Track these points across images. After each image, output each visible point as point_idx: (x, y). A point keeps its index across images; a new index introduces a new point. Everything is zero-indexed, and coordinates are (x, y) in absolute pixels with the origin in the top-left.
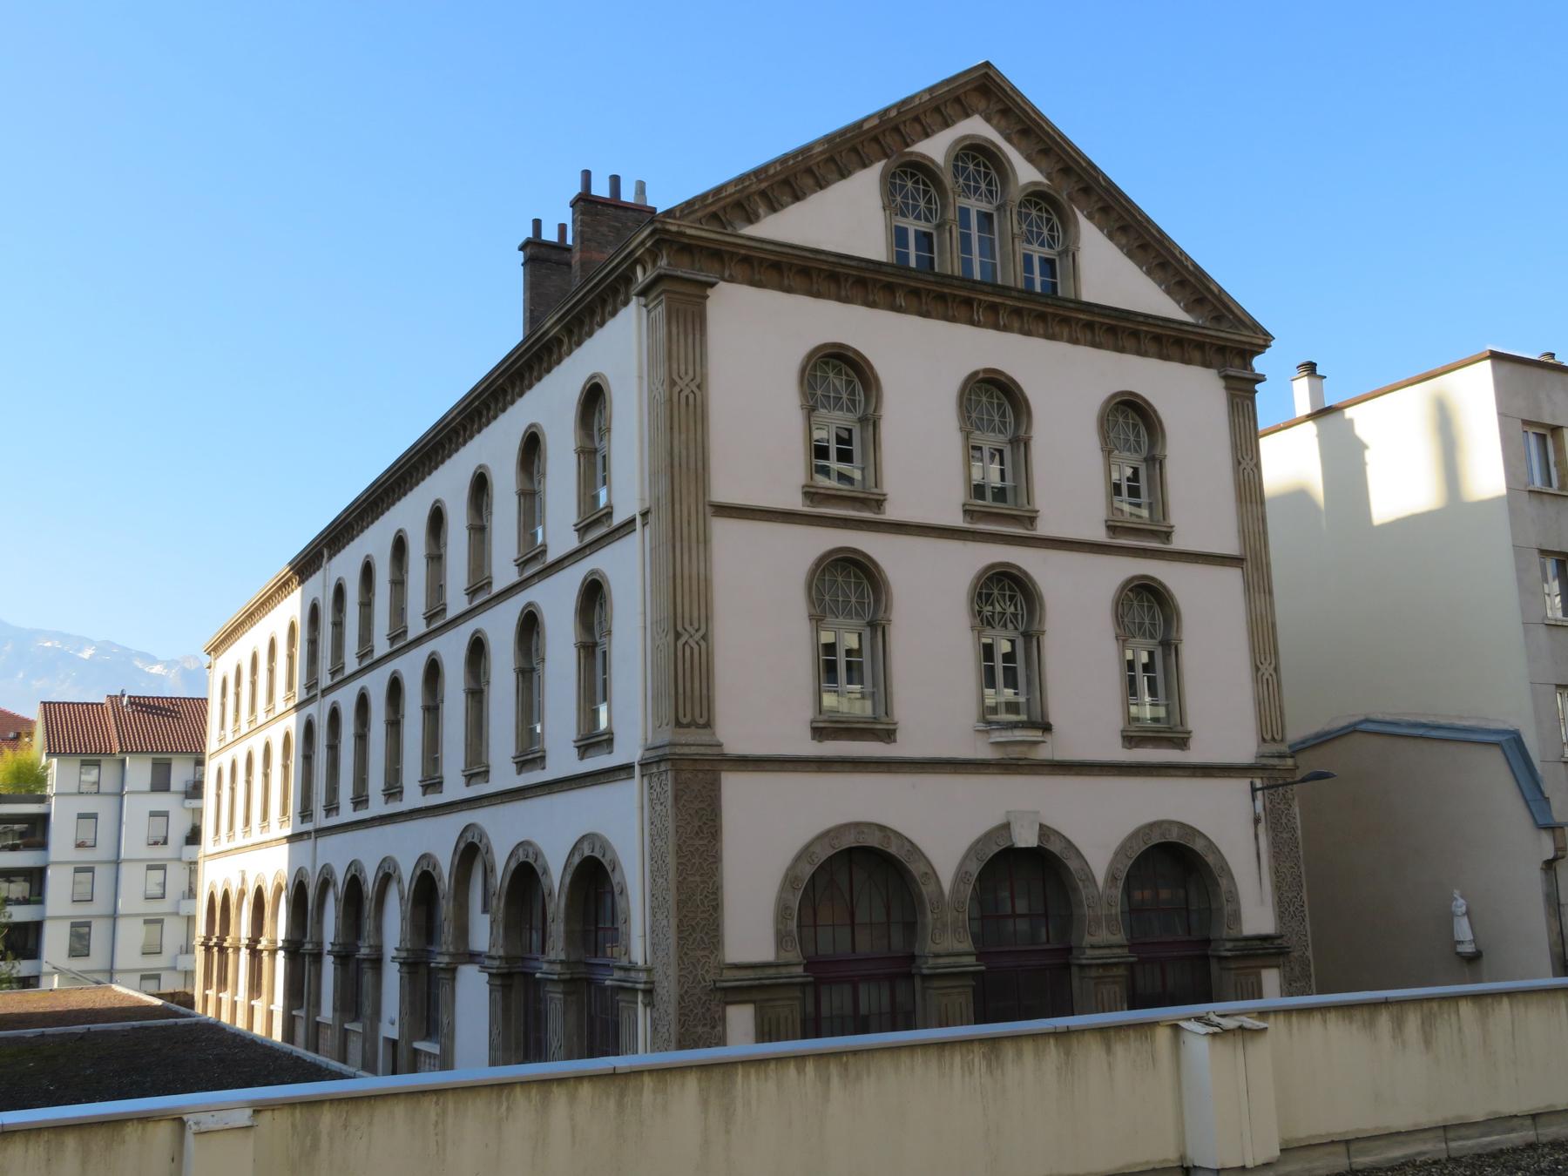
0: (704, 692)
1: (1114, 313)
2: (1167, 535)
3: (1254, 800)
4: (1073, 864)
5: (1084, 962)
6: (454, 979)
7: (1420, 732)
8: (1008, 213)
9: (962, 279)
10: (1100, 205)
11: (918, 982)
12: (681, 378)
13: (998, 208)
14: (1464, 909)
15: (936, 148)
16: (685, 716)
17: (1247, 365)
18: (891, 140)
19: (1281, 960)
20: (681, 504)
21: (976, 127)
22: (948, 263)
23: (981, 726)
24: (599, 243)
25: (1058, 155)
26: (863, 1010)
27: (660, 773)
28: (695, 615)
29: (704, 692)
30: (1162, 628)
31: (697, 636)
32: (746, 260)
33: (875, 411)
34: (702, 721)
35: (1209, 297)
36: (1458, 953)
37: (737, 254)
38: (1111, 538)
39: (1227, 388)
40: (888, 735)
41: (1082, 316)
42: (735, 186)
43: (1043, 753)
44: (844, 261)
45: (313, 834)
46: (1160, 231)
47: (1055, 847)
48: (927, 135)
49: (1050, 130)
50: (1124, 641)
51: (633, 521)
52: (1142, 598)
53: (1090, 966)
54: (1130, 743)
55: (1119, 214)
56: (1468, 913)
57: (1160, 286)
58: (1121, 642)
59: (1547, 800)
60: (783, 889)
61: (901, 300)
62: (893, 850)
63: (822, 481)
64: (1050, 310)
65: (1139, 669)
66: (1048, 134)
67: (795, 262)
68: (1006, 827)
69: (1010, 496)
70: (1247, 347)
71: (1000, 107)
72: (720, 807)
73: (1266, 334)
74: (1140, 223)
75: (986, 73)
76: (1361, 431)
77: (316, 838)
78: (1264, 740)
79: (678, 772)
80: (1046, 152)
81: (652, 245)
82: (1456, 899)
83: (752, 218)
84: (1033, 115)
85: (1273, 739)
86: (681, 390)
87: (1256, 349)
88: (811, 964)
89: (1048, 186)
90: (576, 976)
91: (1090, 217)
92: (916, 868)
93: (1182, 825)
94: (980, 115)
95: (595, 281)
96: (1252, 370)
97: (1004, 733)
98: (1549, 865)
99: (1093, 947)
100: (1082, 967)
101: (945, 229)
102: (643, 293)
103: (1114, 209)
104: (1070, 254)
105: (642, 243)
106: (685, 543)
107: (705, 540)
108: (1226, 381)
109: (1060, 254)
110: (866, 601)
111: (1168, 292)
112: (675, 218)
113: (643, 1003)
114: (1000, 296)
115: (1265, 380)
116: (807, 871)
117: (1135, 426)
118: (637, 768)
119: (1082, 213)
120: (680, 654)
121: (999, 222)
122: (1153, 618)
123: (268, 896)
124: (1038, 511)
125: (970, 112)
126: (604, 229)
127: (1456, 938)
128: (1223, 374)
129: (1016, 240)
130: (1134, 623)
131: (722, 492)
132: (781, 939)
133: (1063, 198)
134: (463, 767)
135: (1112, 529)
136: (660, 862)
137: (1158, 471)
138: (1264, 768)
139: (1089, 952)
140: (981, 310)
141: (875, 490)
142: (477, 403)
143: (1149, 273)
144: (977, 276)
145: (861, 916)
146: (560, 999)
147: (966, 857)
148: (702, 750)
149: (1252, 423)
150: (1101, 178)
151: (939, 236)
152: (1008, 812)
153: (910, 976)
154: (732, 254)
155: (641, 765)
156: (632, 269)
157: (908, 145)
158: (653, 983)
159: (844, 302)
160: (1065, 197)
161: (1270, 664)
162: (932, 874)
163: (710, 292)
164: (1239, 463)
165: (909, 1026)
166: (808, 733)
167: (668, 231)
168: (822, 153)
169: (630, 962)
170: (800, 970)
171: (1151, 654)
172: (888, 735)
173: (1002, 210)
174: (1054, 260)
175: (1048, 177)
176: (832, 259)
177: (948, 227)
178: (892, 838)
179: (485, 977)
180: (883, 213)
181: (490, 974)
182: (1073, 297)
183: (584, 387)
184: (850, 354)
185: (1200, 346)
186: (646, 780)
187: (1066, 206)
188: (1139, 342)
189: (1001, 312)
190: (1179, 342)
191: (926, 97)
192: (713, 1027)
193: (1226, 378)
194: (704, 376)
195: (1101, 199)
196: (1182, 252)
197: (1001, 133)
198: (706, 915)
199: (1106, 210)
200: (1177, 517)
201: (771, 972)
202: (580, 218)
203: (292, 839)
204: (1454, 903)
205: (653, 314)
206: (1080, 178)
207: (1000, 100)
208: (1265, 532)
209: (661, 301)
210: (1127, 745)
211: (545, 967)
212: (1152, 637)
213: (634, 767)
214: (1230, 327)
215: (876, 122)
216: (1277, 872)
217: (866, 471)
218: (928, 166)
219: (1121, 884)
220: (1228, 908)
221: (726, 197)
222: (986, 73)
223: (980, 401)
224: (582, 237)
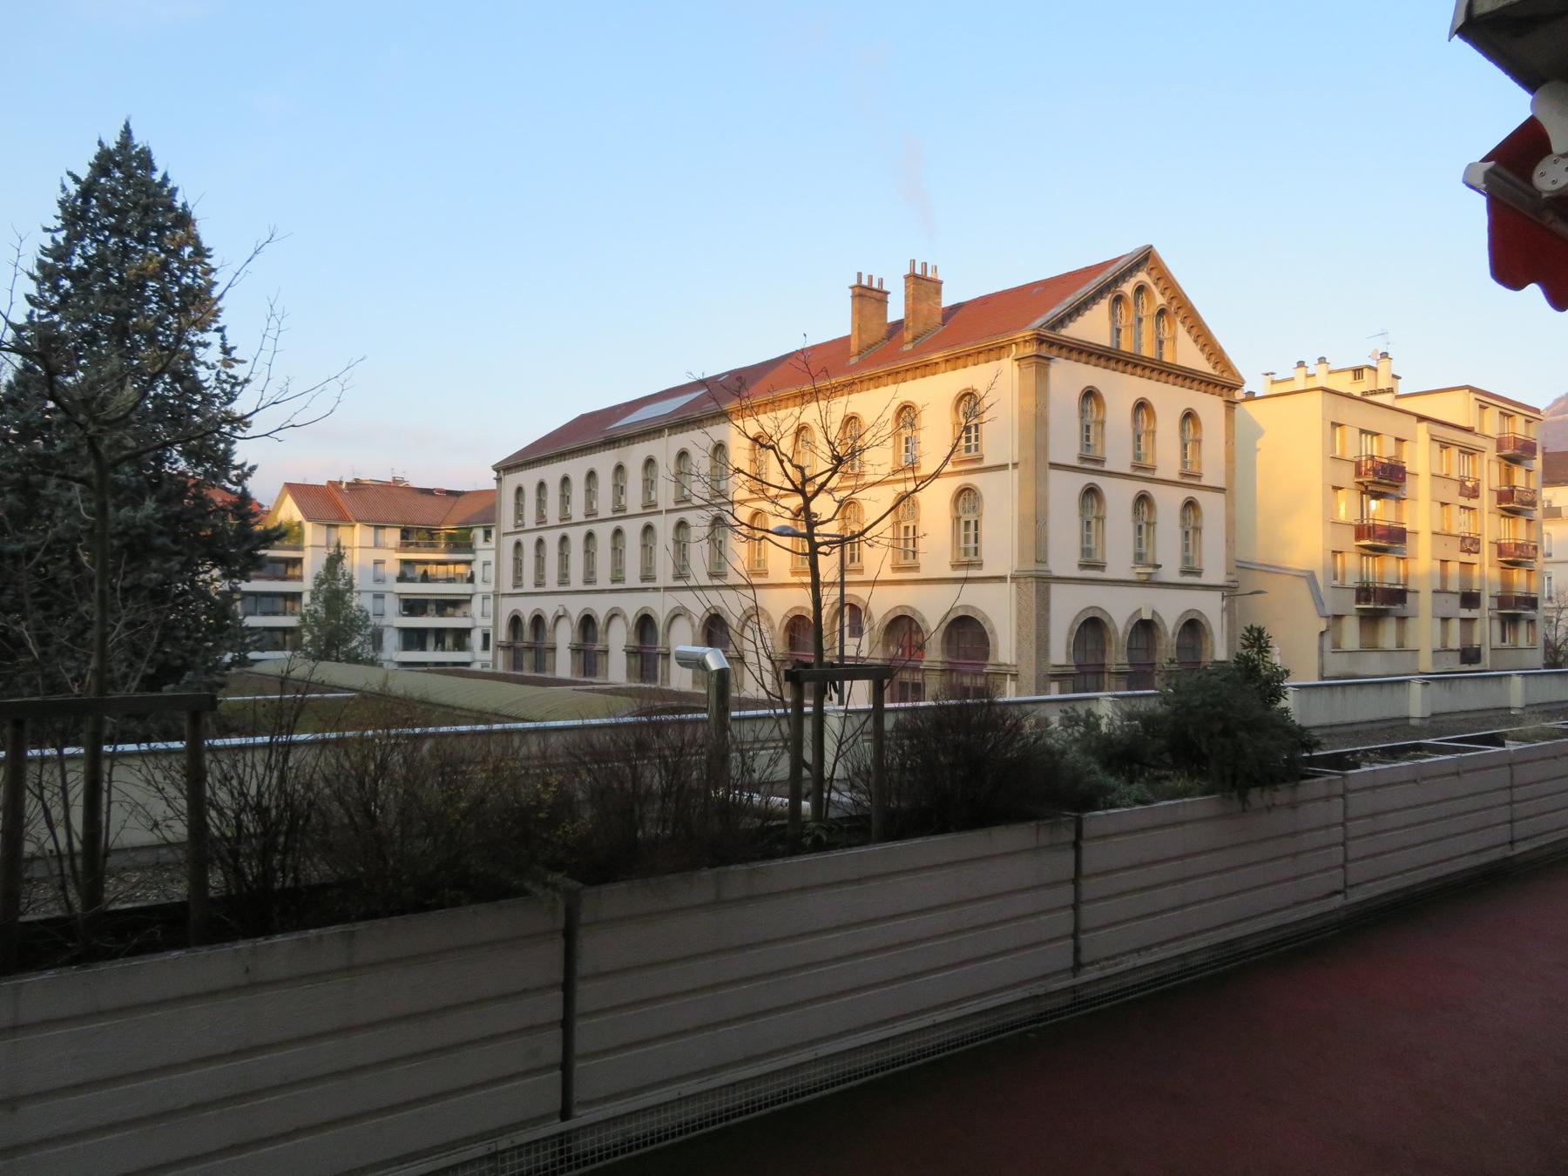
11: (1106, 676)
15: (1128, 288)
22: (1126, 346)
39: (1227, 407)
47: (1156, 620)
56: (1279, 654)
59: (1323, 604)
68: (1140, 610)
79: (1037, 582)
88: (1078, 666)
98: (1322, 634)
118: (1009, 579)
126: (922, 293)
138: (1227, 587)
145: (1088, 648)
148: (1044, 573)
162: (1116, 630)
170: (1074, 668)
186: (1014, 585)
201: (1065, 669)
211: (925, 663)
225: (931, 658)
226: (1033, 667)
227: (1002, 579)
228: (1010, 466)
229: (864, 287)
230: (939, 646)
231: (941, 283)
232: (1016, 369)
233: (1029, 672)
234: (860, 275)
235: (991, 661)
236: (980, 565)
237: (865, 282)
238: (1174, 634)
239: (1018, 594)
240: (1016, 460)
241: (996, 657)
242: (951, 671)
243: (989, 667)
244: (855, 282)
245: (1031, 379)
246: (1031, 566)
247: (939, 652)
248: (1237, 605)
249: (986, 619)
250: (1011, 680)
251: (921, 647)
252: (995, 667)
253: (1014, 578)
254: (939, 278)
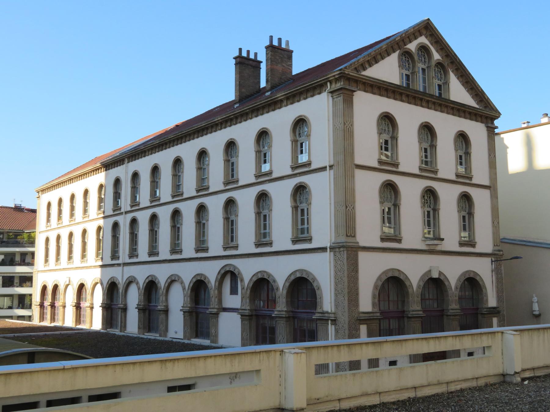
1: (460, 105)
2: (470, 178)
3: (492, 264)
4: (446, 283)
5: (449, 314)
6: (218, 317)
7: (524, 243)
8: (431, 69)
9: (423, 93)
10: (456, 68)
11: (406, 319)
12: (346, 122)
13: (428, 67)
14: (537, 300)
15: (412, 46)
16: (349, 233)
17: (493, 123)
18: (401, 44)
19: (498, 315)
21: (423, 40)
23: (424, 239)
24: (276, 62)
25: (446, 50)
26: (391, 327)
27: (340, 251)
30: (433, 204)
31: (352, 208)
32: (364, 83)
33: (397, 135)
34: (353, 235)
35: (484, 100)
36: (533, 315)
37: (362, 81)
38: (421, 173)
39: (488, 130)
40: (399, 241)
41: (452, 105)
42: (363, 59)
43: (439, 248)
44: (391, 85)
45: (122, 265)
46: (472, 77)
47: (442, 278)
48: (410, 42)
49: (444, 42)
50: (460, 212)
51: (326, 167)
52: (388, 188)
53: (450, 315)
56: (537, 302)
57: (470, 95)
58: (459, 213)
60: (374, 289)
61: (404, 98)
62: (401, 277)
63: (383, 158)
64: (443, 103)
65: (386, 213)
66: (443, 43)
67: (378, 85)
68: (430, 271)
69: (429, 163)
70: (494, 117)
71: (430, 33)
72: (358, 262)
73: (500, 113)
75: (428, 22)
76: (506, 142)
77: (123, 266)
78: (495, 245)
79: (348, 251)
80: (442, 49)
81: (338, 77)
82: (534, 297)
83: (365, 69)
84: (440, 37)
85: (497, 245)
86: (347, 126)
87: (496, 118)
88: (382, 313)
89: (442, 61)
90: (290, 316)
91: (453, 72)
92: (407, 283)
93: (474, 272)
94: (424, 35)
95: (308, 84)
96: (494, 125)
97: (431, 241)
99: (452, 309)
100: (447, 315)
101: (414, 74)
102: (332, 92)
103: (460, 70)
104: (447, 84)
105: (334, 76)
107: (353, 177)
109: (443, 83)
110: (392, 197)
111: (473, 97)
112: (347, 69)
113: (331, 324)
114: (431, 98)
115: (498, 128)
116: (380, 283)
117: (388, 125)
118: (328, 249)
119: (451, 70)
120: (347, 213)
121: (428, 72)
122: (466, 205)
123: (61, 288)
124: (473, 176)
125: (422, 35)
127: (533, 309)
128: (487, 126)
129: (434, 79)
130: (385, 197)
131: (358, 161)
132: (374, 305)
133: (446, 65)
134: (222, 244)
135: (458, 176)
136: (340, 279)
137: (469, 157)
138: (495, 254)
139: (451, 311)
140: (424, 102)
141: (396, 161)
142: (232, 117)
143: (468, 91)
144: (404, 85)
145: (390, 299)
146: (284, 323)
147: (420, 281)
148: (354, 244)
150: (457, 59)
151: (412, 76)
152: (431, 267)
153: (403, 317)
154: (360, 81)
155: (330, 248)
156: (326, 83)
157: (405, 45)
158: (336, 317)
159: (417, 106)
160: (446, 64)
161: (497, 221)
162: (411, 285)
163: (354, 93)
164: (490, 155)
165: (477, 328)
166: (379, 240)
167: (345, 73)
168: (385, 48)
169: (323, 311)
170: (378, 314)
171: (389, 209)
172: (399, 241)
173: (429, 68)
174: (409, 75)
175: (442, 58)
176: (388, 84)
177: (415, 74)
179: (239, 316)
180: (398, 68)
181: (241, 315)
182: (448, 98)
183: (296, 119)
184: (390, 115)
185: (481, 116)
186: (332, 253)
187: (446, 67)
188: (365, 86)
189: (430, 103)
190: (476, 115)
191: (412, 30)
192: (357, 331)
193: (487, 127)
194: (353, 122)
195: (456, 65)
196: (478, 85)
197: (430, 42)
198: (355, 296)
200: (474, 172)
201: (372, 315)
202: (270, 53)
203: (102, 266)
204: (533, 298)
205: (335, 99)
206: (451, 59)
207: (431, 31)
208: (496, 178)
209: (341, 96)
210: (460, 246)
211: (276, 313)
212: (465, 211)
213: (327, 248)
214: (489, 110)
216: (497, 287)
217: (393, 155)
218: (410, 53)
219: (458, 290)
220: (485, 298)
221: (360, 62)
222: (428, 22)
223: (382, 123)
224: (271, 60)
225: (278, 309)
226: (346, 314)
227: (323, 249)
228: (328, 168)
229: (244, 58)
230: (284, 300)
231: (292, 52)
232: (331, 99)
233: (344, 319)
234: (240, 50)
235: (319, 310)
236: (310, 240)
237: (244, 54)
238: (456, 288)
239: (335, 260)
240: (332, 163)
241: (321, 307)
242: (294, 318)
243: (317, 315)
244: (237, 54)
245: (341, 106)
246: (343, 239)
247: (284, 305)
248: (503, 268)
249: (314, 279)
250: (332, 324)
251: (274, 301)
252: (320, 315)
253: (332, 248)
254: (291, 48)
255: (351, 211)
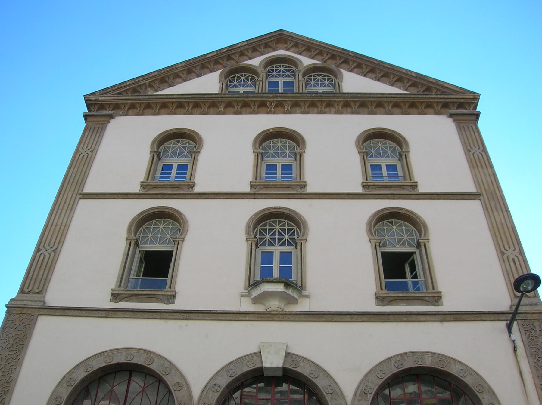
0: (45, 276)
20: (63, 196)
28: (53, 241)
29: (45, 276)
54: (382, 302)
55: (365, 65)
74: (378, 65)
106: (59, 211)
108: (453, 118)
120: (37, 258)
133: (333, 67)
149: (477, 134)
161: (515, 250)
166: (109, 296)
167: (90, 100)
178: (156, 359)
193: (451, 116)
196: (406, 70)
199: (359, 66)
210: (380, 303)
215: (215, 54)
255: (47, 256)
